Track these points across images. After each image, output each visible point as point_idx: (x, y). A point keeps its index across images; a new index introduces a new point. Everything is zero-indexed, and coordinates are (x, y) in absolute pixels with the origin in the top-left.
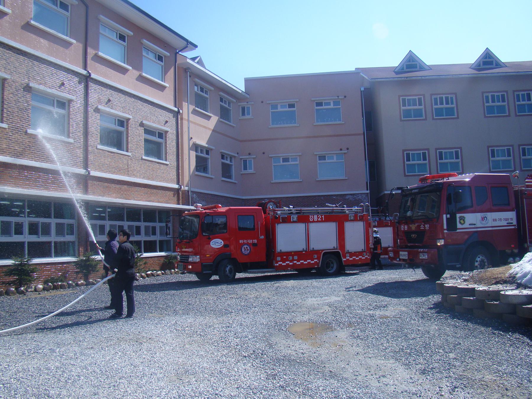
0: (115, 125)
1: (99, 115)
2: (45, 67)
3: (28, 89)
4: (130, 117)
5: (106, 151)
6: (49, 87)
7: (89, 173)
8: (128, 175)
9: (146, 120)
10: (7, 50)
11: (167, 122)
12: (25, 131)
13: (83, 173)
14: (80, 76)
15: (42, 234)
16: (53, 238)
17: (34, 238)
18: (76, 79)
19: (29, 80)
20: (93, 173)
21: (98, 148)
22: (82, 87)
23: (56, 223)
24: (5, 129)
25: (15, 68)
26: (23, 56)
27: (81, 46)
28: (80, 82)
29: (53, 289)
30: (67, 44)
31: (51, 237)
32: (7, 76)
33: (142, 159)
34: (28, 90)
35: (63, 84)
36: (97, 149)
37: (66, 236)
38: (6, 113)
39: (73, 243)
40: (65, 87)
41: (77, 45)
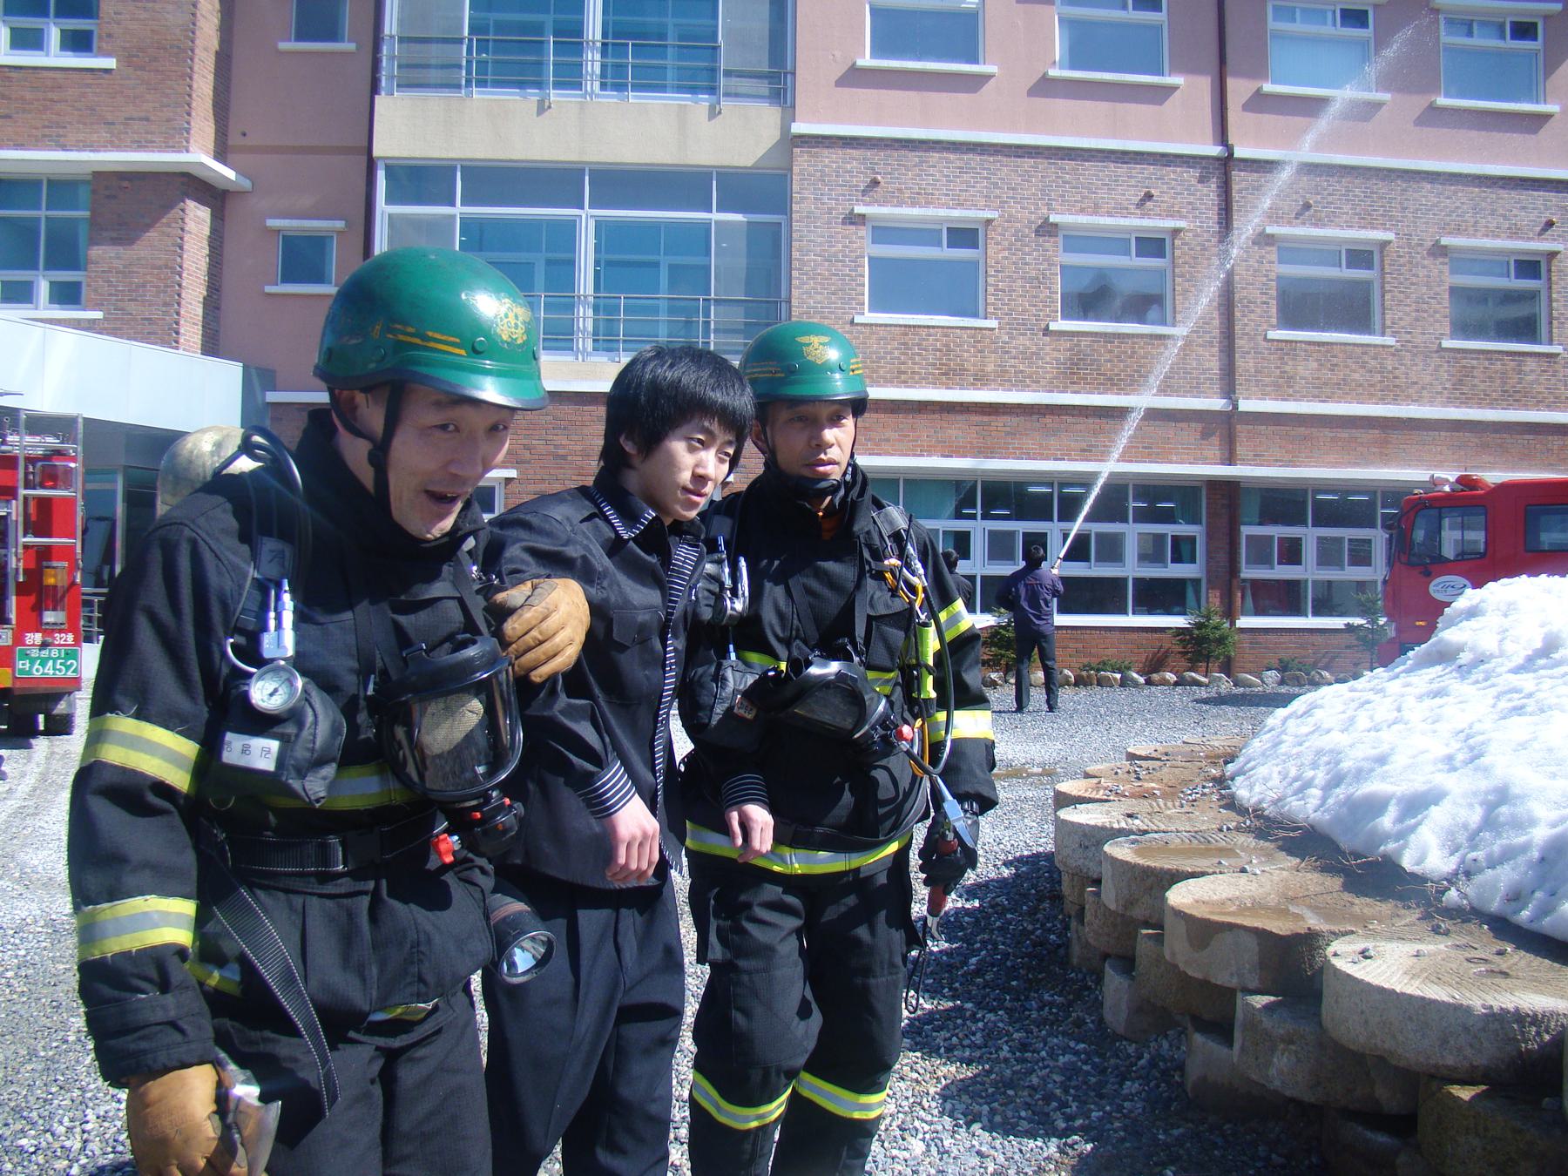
0: (1340, 266)
1: (1274, 249)
2: (1092, 166)
3: (1047, 229)
4: (1390, 236)
5: (1301, 342)
6: (1108, 213)
7: (1235, 407)
8: (1382, 400)
9: (1458, 231)
10: (991, 155)
11: (1550, 224)
12: (1043, 327)
13: (1218, 408)
14: (1204, 162)
15: (1096, 560)
16: (1308, 571)
17: (1078, 570)
18: (1191, 175)
19: (1049, 209)
20: (1245, 405)
21: (1268, 337)
22: (1209, 193)
23: (1318, 538)
24: (992, 329)
25: (1013, 189)
26: (1033, 158)
27: (1203, 85)
28: (1205, 177)
29: (1076, 684)
30: (1160, 94)
31: (1124, 566)
32: (988, 215)
33: (1441, 349)
34: (1048, 232)
35: (1149, 196)
36: (1265, 339)
37: (1276, 566)
38: (993, 295)
39: (1196, 582)
40: (1157, 201)
41: (1193, 89)
